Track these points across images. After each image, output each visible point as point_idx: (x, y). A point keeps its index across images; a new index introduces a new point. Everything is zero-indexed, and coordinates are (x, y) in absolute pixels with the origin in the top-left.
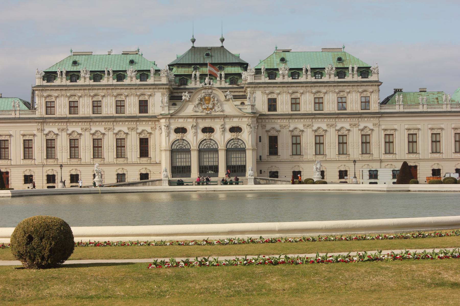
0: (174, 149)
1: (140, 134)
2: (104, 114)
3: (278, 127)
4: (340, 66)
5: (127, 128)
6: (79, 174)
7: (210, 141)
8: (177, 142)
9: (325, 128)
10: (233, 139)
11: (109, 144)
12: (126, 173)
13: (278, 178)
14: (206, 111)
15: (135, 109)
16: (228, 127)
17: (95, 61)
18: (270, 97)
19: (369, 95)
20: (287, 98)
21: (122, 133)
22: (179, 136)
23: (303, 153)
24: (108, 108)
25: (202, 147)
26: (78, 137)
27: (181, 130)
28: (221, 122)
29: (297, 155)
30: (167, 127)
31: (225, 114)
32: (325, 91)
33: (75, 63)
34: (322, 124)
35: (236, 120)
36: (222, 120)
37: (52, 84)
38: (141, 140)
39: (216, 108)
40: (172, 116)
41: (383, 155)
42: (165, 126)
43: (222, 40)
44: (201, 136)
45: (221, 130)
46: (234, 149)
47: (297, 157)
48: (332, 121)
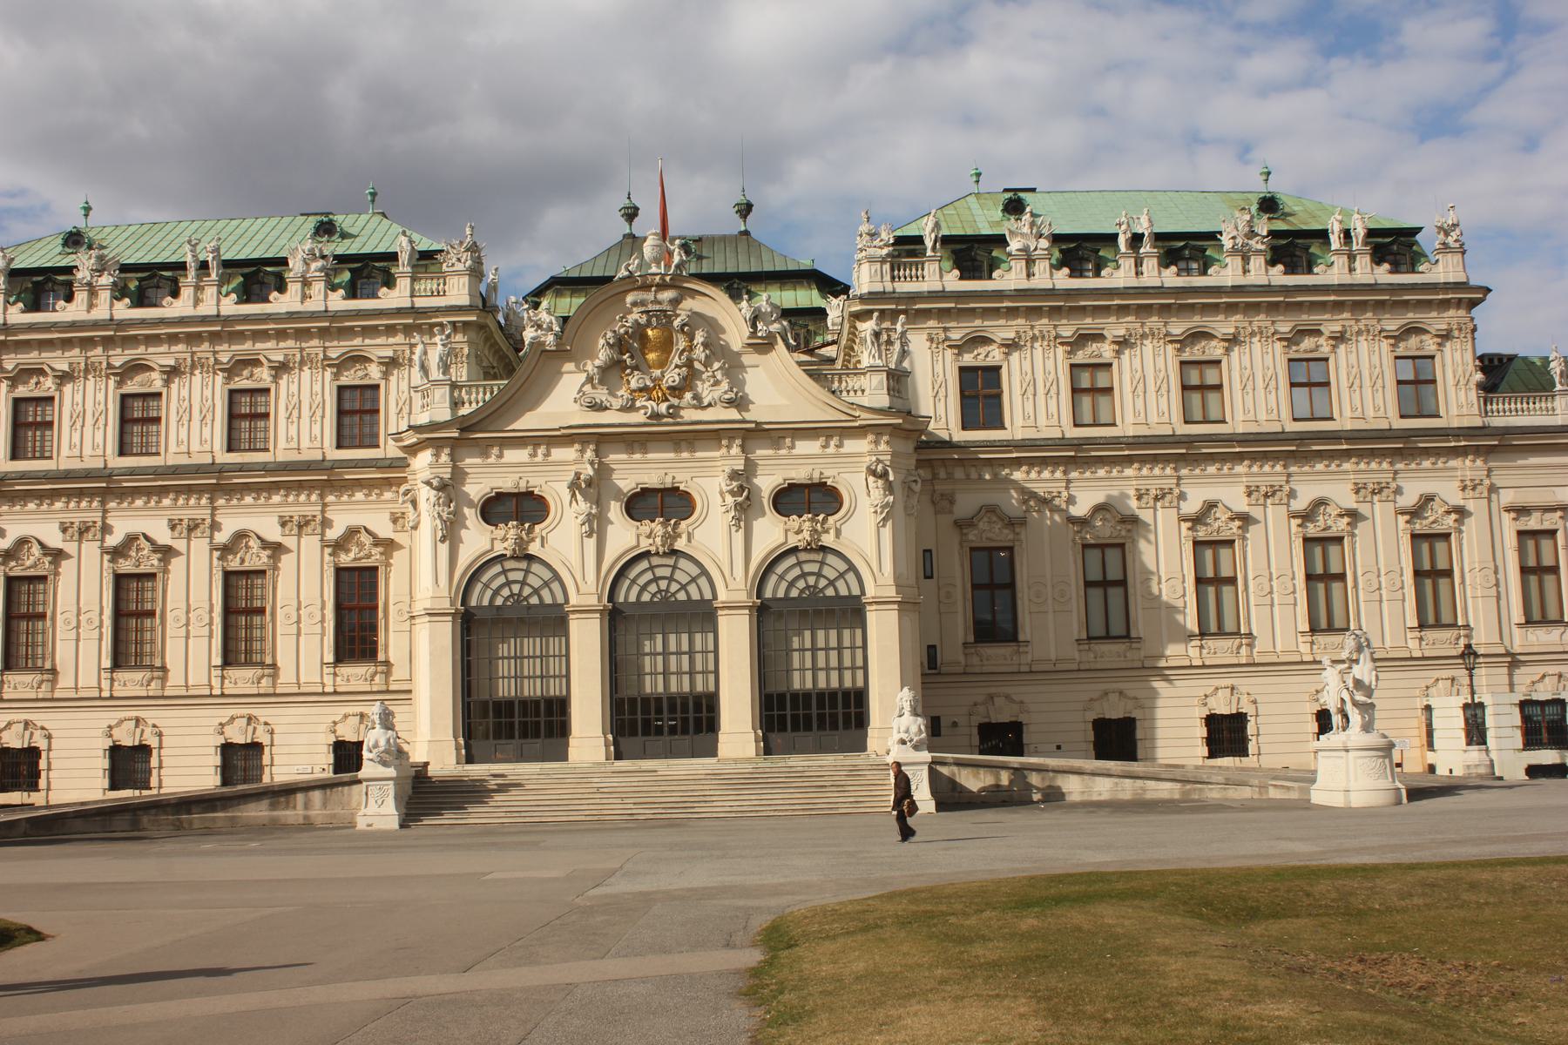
0: (479, 607)
1: (339, 546)
2: (172, 455)
4: (1280, 226)
5: (274, 521)
6: (42, 744)
9: (1241, 504)
10: (794, 550)
11: (190, 596)
15: (317, 429)
17: (171, 237)
18: (968, 359)
19: (1430, 345)
20: (1050, 364)
21: (254, 544)
22: (503, 538)
23: (1140, 627)
24: (192, 426)
25: (629, 594)
26: (45, 567)
27: (518, 508)
28: (729, 458)
29: (1108, 637)
30: (443, 487)
31: (748, 416)
34: (1227, 489)
35: (805, 447)
36: (735, 450)
38: (339, 572)
40: (467, 435)
41: (1516, 631)
42: (428, 483)
43: (745, 210)
44: (624, 535)
45: (730, 500)
46: (801, 610)
47: (1109, 652)
48: (1271, 473)
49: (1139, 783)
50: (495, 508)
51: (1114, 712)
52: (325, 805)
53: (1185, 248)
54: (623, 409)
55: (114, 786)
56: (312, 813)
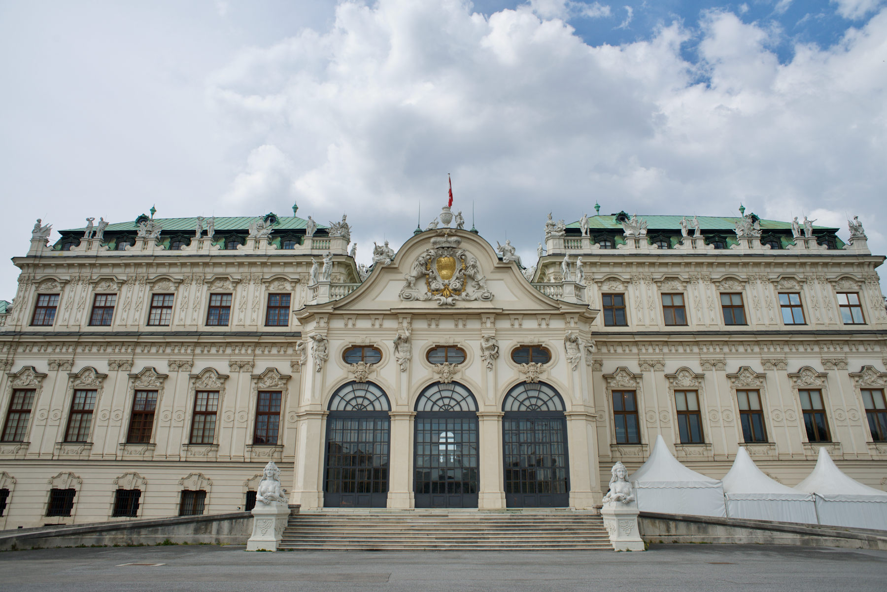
3: (635, 368)
7: (452, 387)
8: (349, 389)
10: (524, 383)
12: (207, 489)
14: (443, 299)
16: (506, 346)
18: (606, 288)
24: (189, 310)
25: (425, 406)
28: (489, 327)
32: (743, 276)
33: (143, 219)
37: (65, 253)
39: (470, 289)
40: (337, 310)
42: (313, 338)
44: (424, 373)
49: (768, 533)
52: (230, 531)
53: (718, 237)
54: (426, 300)
55: (116, 514)
56: (221, 537)
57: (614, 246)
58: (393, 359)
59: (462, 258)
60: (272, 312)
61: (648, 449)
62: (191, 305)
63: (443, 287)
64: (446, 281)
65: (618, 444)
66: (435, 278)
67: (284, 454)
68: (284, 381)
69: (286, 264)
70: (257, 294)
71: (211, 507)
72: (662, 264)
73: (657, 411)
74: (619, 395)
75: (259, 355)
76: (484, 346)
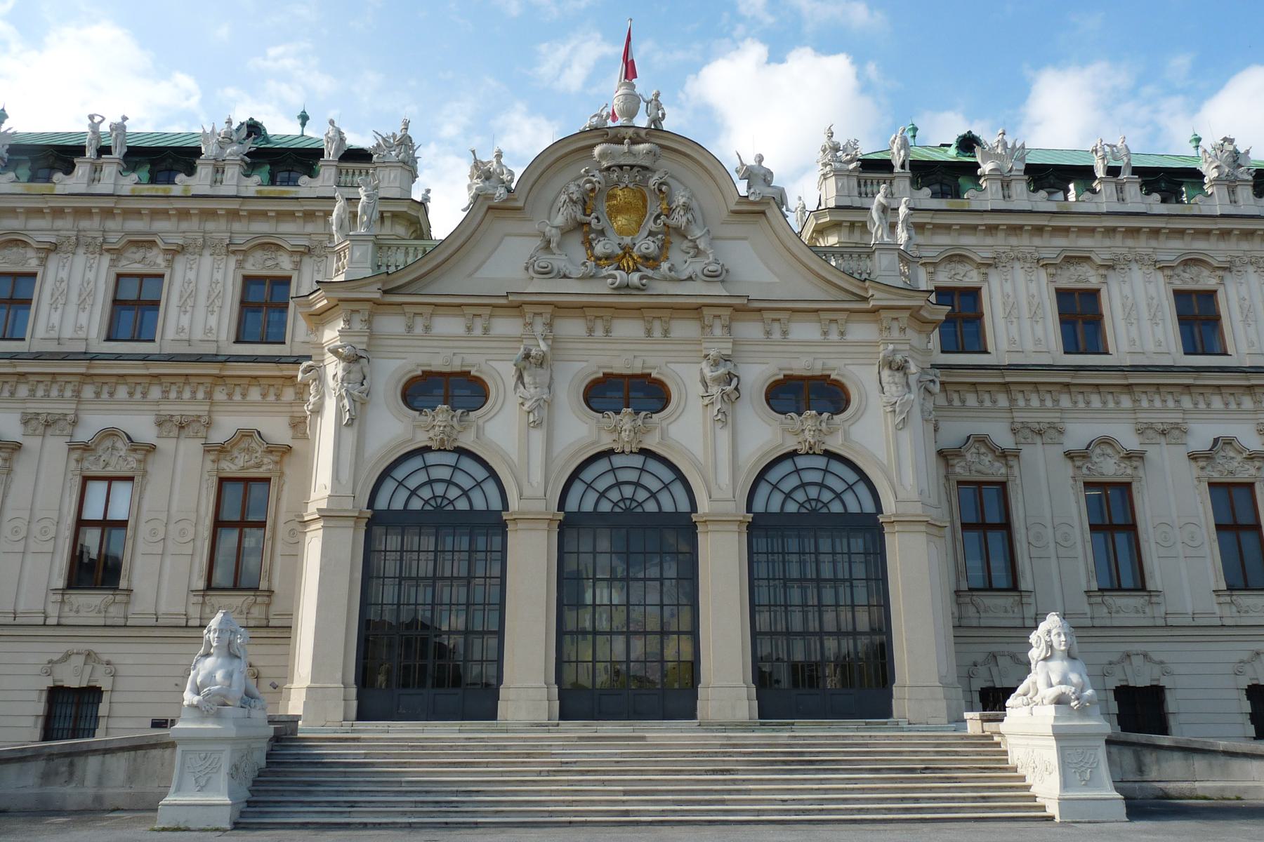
3: (1002, 437)
12: (104, 683)
13: (1164, 730)
16: (757, 374)
35: (805, 331)
39: (676, 256)
45: (715, 390)
50: (422, 390)
51: (1142, 680)
52: (131, 778)
57: (958, 195)
58: (513, 400)
59: (662, 192)
60: (250, 316)
61: (1032, 600)
62: (74, 297)
63: (620, 252)
64: (627, 240)
65: (971, 590)
66: (602, 233)
67: (274, 609)
68: (275, 458)
69: (281, 216)
70: (218, 276)
71: (114, 723)
72: (1057, 230)
73: (1049, 525)
74: (969, 490)
75: (222, 403)
76: (708, 373)
